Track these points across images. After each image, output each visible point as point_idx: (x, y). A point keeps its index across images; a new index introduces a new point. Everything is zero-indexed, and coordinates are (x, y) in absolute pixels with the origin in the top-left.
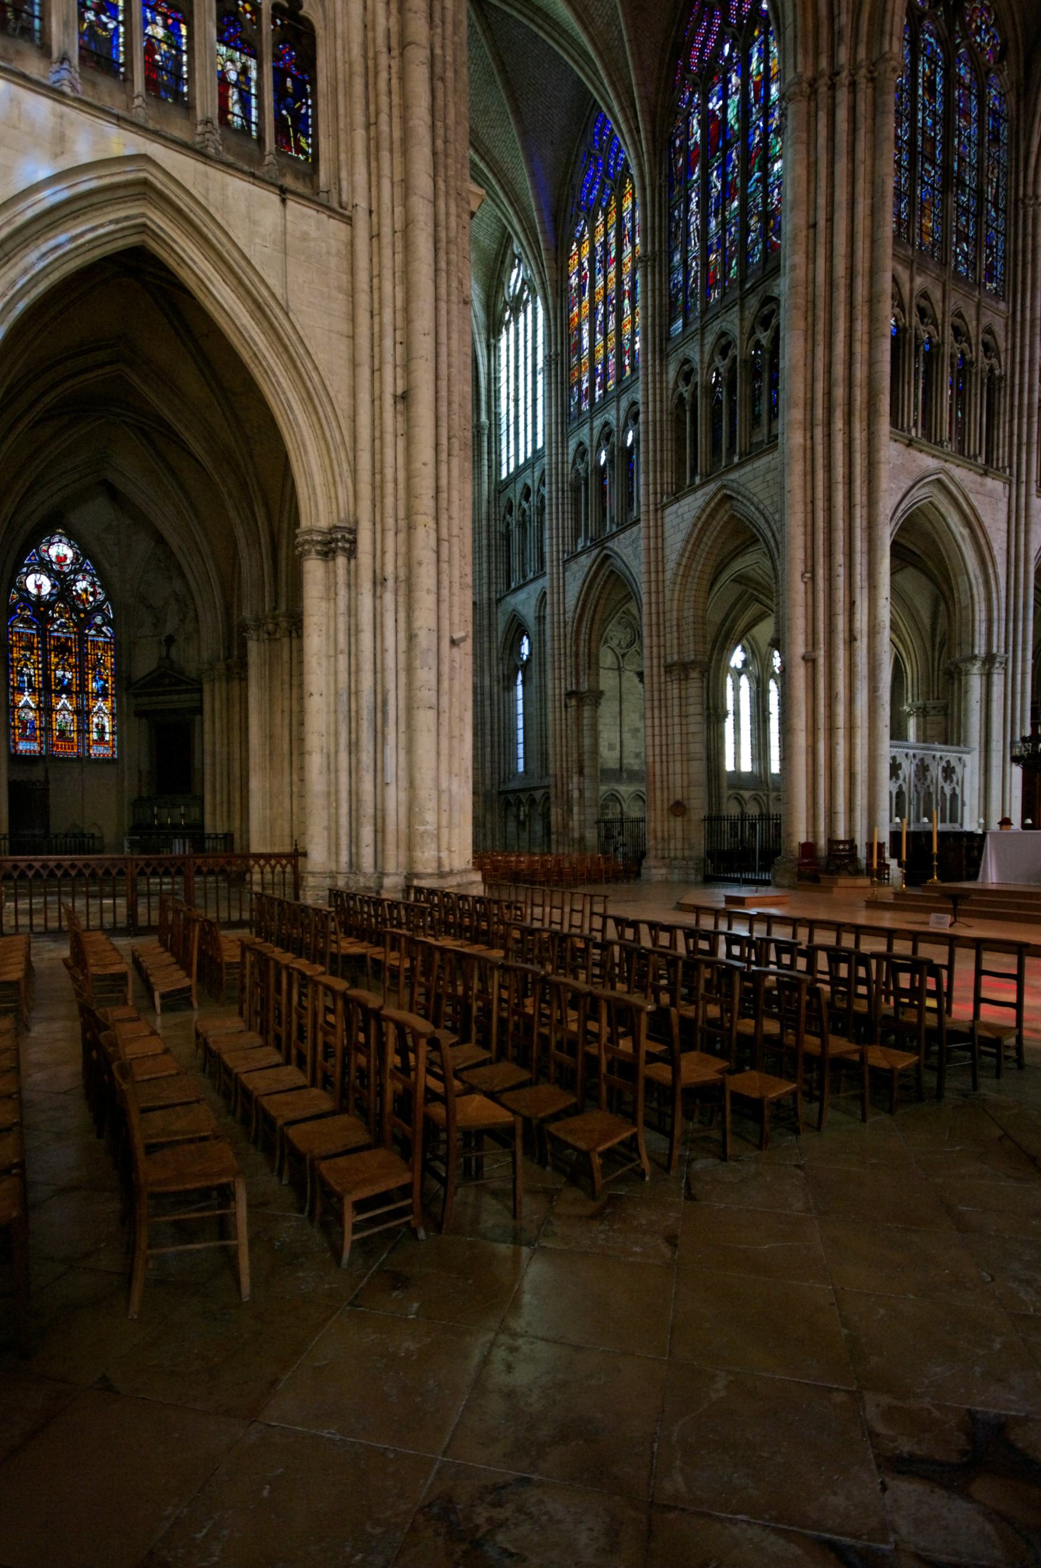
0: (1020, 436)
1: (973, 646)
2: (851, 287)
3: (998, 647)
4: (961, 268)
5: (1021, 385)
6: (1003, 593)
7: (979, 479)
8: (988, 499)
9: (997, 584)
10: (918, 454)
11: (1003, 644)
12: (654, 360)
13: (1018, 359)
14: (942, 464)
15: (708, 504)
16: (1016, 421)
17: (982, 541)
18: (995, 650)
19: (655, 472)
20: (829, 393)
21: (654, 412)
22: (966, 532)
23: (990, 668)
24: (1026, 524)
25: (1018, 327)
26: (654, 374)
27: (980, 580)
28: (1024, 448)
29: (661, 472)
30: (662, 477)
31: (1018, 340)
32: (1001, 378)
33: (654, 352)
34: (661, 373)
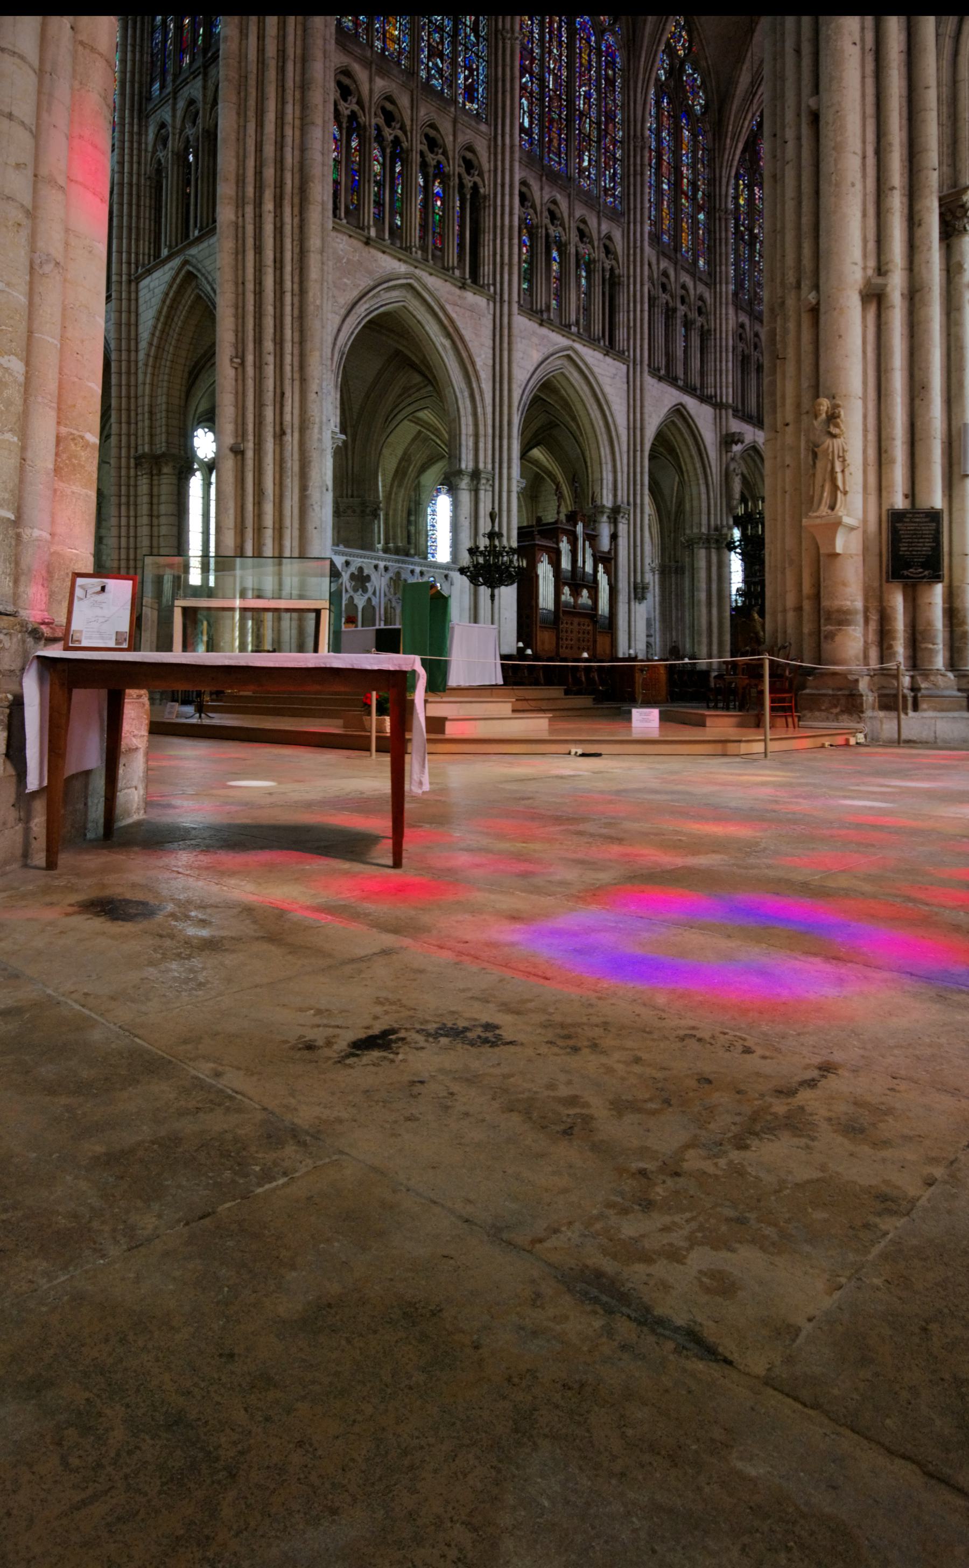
0: (502, 256)
1: (460, 460)
3: (485, 463)
4: (434, 82)
5: (503, 206)
6: (489, 409)
7: (458, 291)
8: (468, 313)
9: (482, 400)
10: (380, 255)
11: (489, 461)
12: (132, 118)
13: (499, 181)
14: (412, 269)
15: (174, 279)
16: (498, 241)
17: (464, 355)
18: (481, 466)
19: (130, 238)
21: (131, 173)
22: (447, 343)
23: (478, 483)
24: (510, 343)
25: (499, 150)
26: (131, 133)
27: (466, 394)
28: (506, 269)
29: (137, 240)
30: (137, 246)
31: (499, 163)
32: (485, 197)
33: (132, 111)
34: (140, 134)
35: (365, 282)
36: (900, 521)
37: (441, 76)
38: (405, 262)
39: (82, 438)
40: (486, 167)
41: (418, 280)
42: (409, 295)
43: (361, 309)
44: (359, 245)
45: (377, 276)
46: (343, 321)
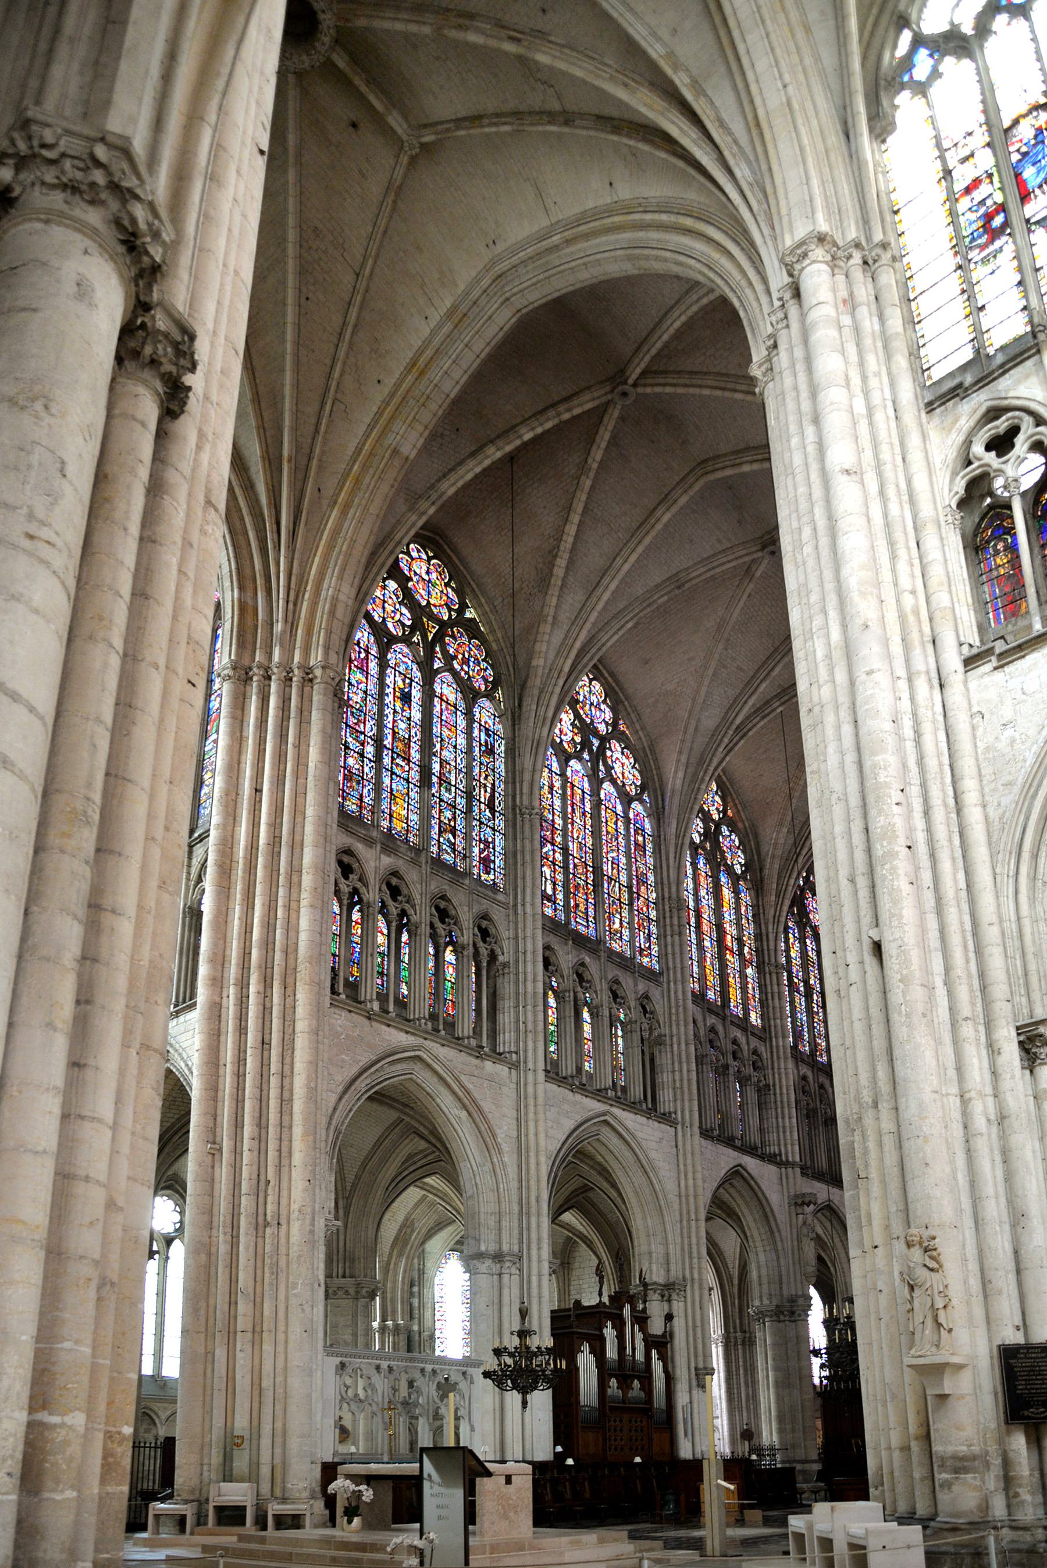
4: (446, 856)
36: (1015, 1357)
37: (454, 850)
38: (413, 1034)
39: (119, 1433)
43: (362, 1084)
46: (340, 1099)
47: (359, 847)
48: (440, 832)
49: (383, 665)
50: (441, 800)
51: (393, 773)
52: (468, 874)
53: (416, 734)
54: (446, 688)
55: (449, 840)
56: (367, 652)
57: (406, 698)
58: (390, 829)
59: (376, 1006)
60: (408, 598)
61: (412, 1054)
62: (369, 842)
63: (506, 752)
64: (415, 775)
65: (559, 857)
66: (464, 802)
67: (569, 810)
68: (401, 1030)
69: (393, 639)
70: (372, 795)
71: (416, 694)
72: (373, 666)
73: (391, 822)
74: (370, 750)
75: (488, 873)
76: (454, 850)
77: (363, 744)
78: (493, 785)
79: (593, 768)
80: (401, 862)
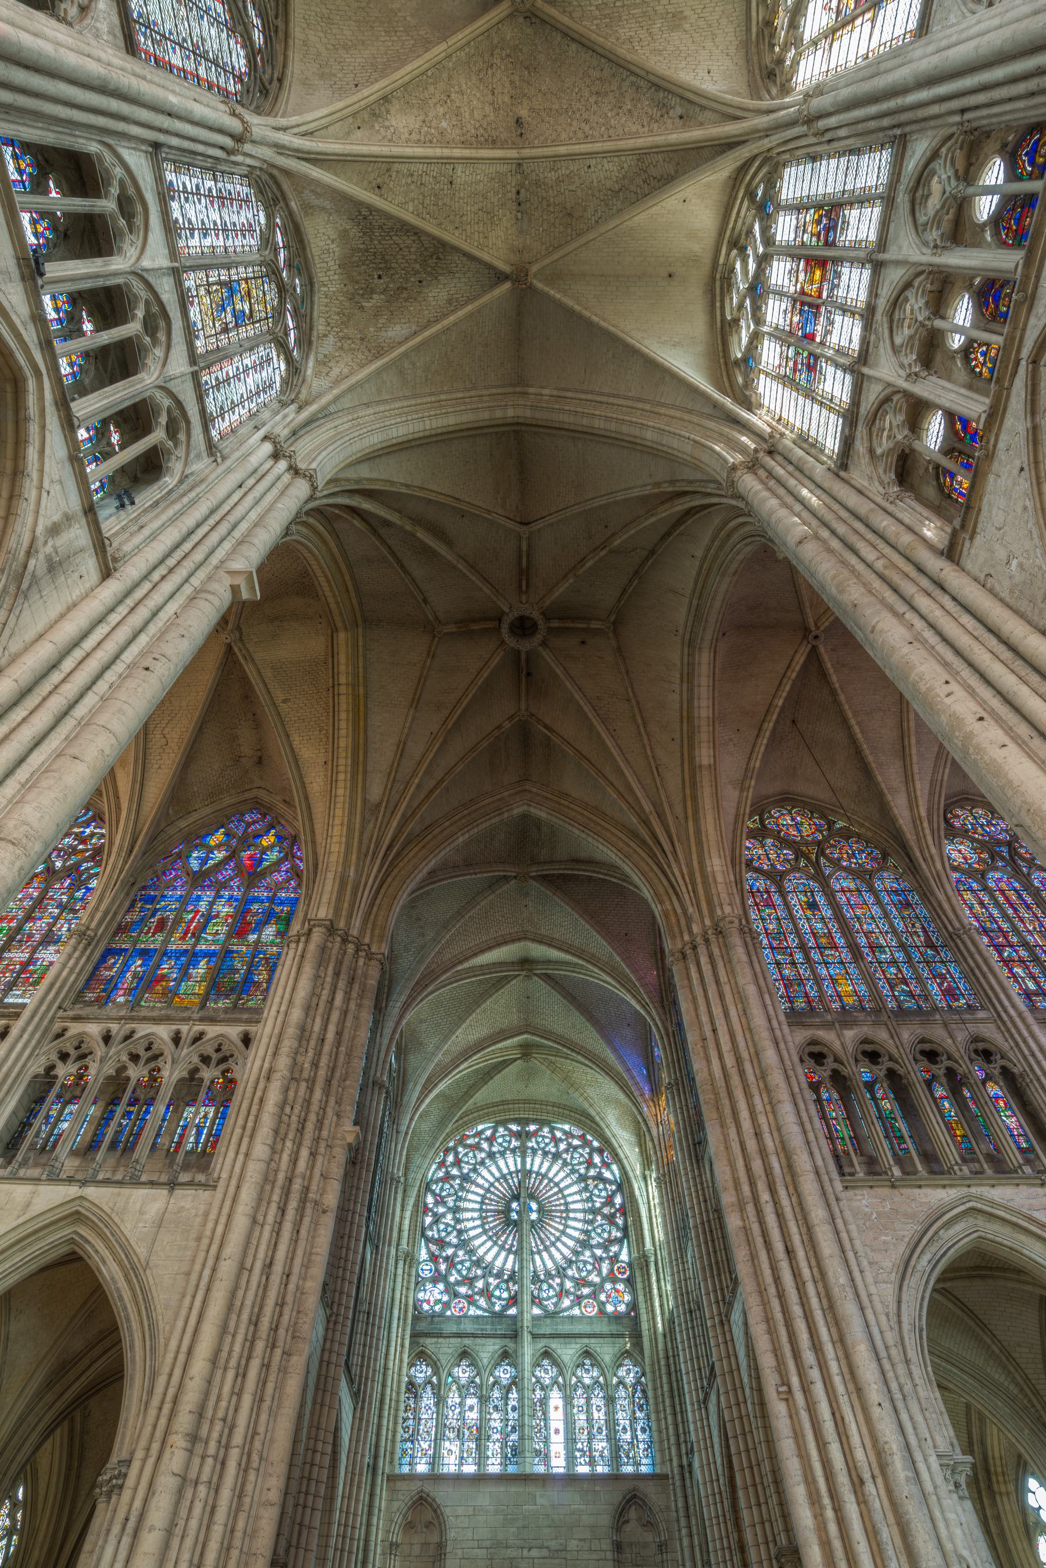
2: (742, 1073)
4: (907, 1005)
10: (917, 1191)
13: (1027, 1052)
14: (964, 1191)
19: (713, 1277)
20: (748, 1169)
21: (701, 1214)
25: (1010, 1025)
26: (694, 1178)
29: (719, 1275)
30: (720, 1281)
31: (1016, 1036)
32: (1021, 1075)
33: (691, 1159)
35: (908, 1230)
37: (913, 996)
38: (952, 1186)
40: (1005, 1046)
41: (979, 1198)
42: (980, 1222)
43: (924, 1262)
44: (886, 1192)
45: (922, 1217)
47: (821, 1034)
48: (892, 989)
49: (783, 894)
50: (880, 963)
51: (826, 963)
52: (936, 1009)
53: (833, 926)
54: (843, 882)
55: (903, 991)
56: (767, 892)
57: (813, 906)
58: (843, 1007)
59: (897, 1172)
60: (784, 842)
61: (962, 1208)
62: (828, 1026)
63: (921, 898)
64: (846, 955)
65: (1023, 953)
66: (902, 954)
67: (1010, 911)
68: (937, 1186)
69: (782, 875)
70: (815, 988)
71: (820, 899)
72: (776, 899)
73: (841, 1001)
74: (799, 957)
75: (958, 1000)
76: (913, 996)
77: (791, 955)
78: (923, 928)
79: (1013, 869)
80: (865, 1029)
